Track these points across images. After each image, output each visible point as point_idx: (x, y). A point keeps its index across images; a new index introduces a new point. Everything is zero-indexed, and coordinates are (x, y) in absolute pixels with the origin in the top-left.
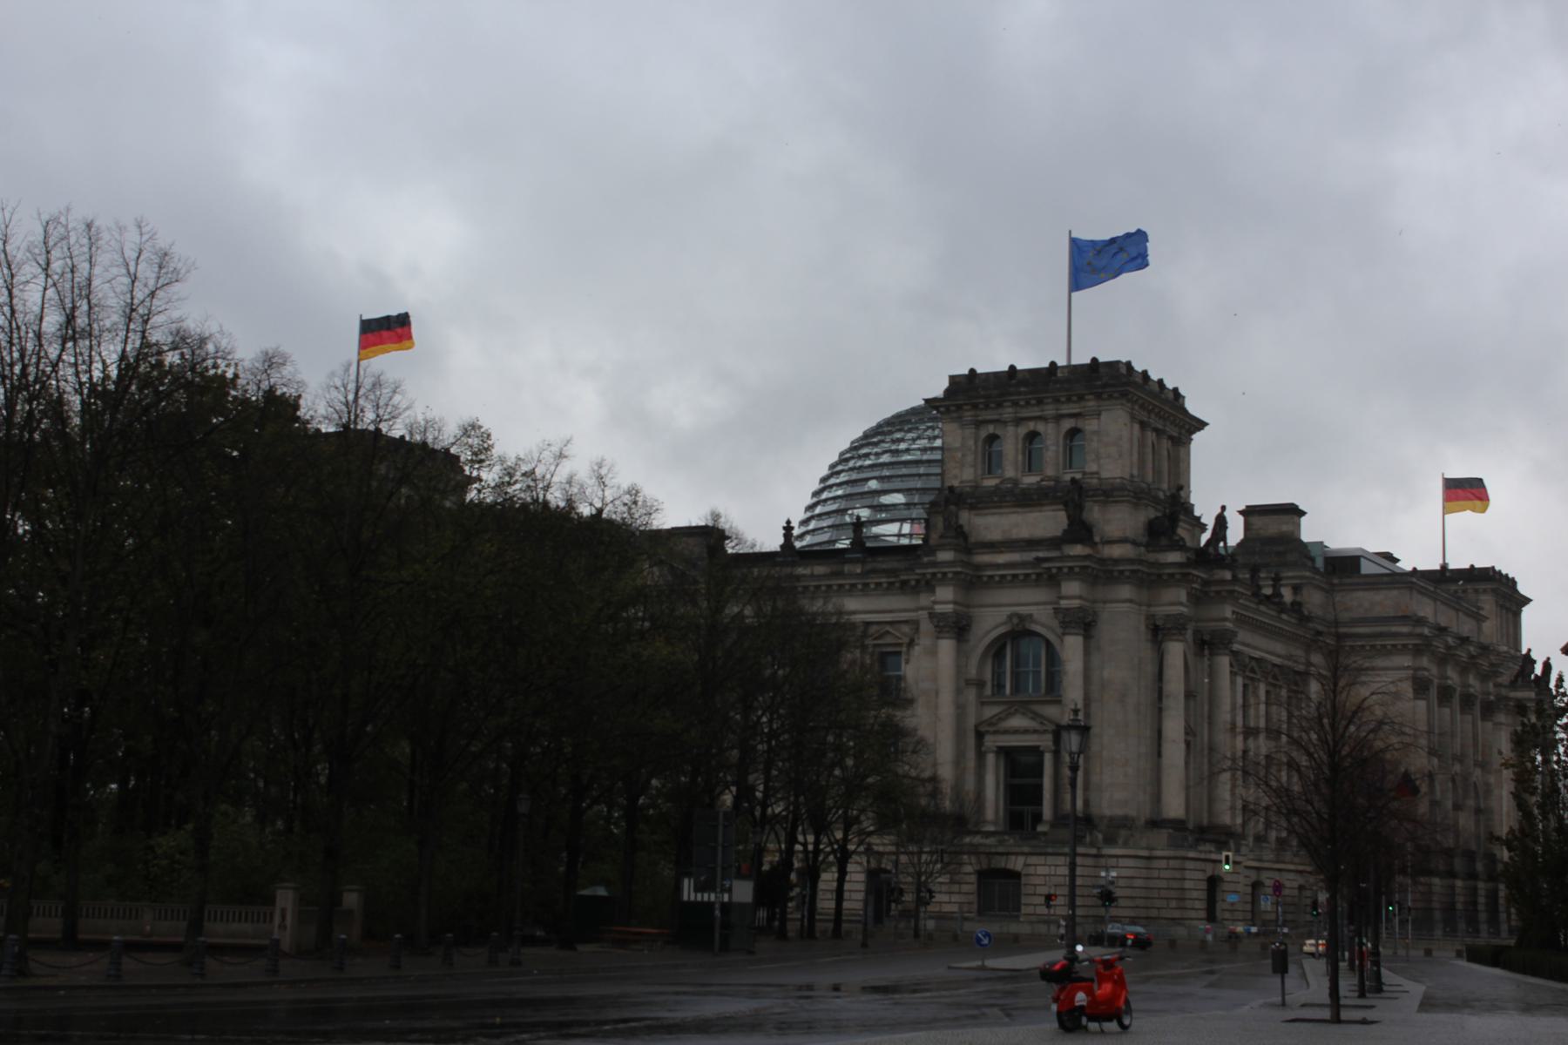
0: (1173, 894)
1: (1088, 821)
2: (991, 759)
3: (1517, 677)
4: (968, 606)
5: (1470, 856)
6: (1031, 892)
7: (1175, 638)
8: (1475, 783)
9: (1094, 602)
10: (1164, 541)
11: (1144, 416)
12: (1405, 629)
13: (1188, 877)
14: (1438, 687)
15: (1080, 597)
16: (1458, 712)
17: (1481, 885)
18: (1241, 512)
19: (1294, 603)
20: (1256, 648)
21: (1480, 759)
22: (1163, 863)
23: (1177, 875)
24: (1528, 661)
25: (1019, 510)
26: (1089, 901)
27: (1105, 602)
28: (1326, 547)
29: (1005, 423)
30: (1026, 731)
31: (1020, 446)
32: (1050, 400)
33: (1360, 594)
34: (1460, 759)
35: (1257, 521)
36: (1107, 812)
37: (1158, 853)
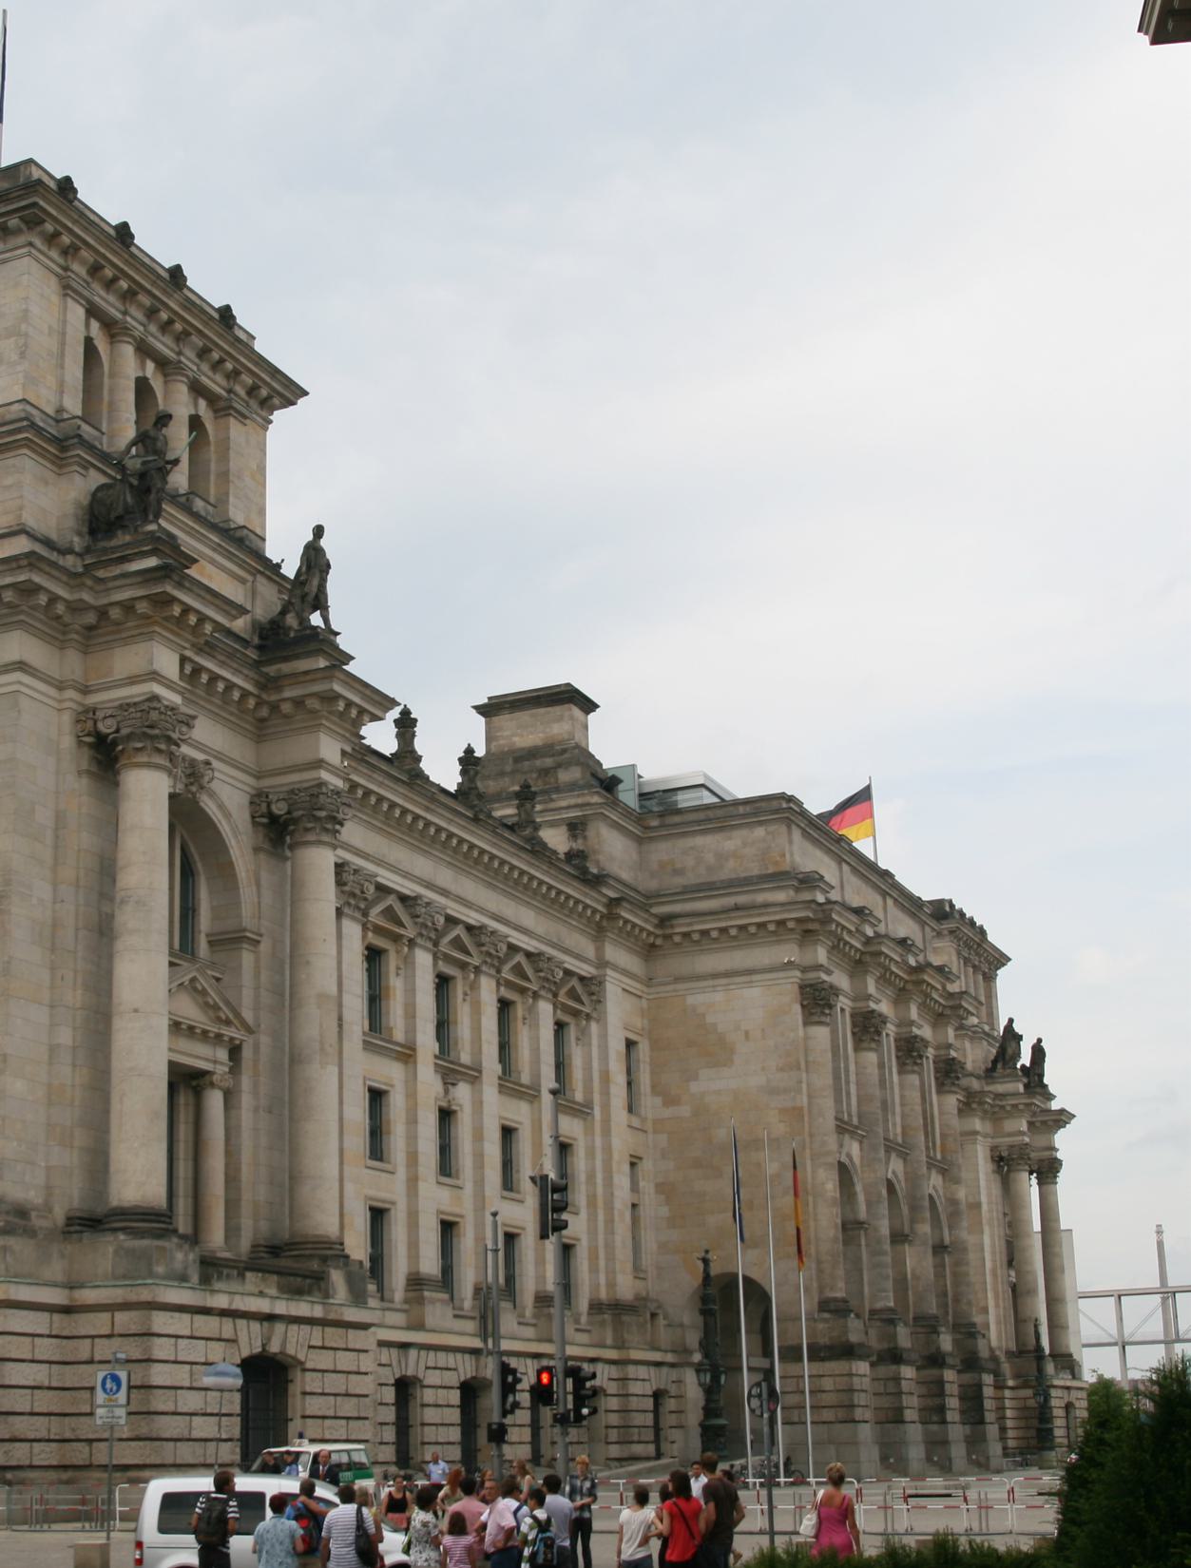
3: (995, 1062)
5: (927, 1325)
7: (143, 758)
8: (930, 1196)
10: (123, 538)
11: (109, 303)
12: (781, 896)
13: (158, 1354)
14: (852, 1016)
16: (895, 1070)
17: (949, 1375)
18: (482, 710)
19: (570, 856)
21: (939, 1157)
22: (100, 1323)
23: (133, 1349)
24: (1012, 1036)
28: (640, 777)
33: (699, 841)
34: (901, 1149)
35: (506, 721)
37: (88, 1296)
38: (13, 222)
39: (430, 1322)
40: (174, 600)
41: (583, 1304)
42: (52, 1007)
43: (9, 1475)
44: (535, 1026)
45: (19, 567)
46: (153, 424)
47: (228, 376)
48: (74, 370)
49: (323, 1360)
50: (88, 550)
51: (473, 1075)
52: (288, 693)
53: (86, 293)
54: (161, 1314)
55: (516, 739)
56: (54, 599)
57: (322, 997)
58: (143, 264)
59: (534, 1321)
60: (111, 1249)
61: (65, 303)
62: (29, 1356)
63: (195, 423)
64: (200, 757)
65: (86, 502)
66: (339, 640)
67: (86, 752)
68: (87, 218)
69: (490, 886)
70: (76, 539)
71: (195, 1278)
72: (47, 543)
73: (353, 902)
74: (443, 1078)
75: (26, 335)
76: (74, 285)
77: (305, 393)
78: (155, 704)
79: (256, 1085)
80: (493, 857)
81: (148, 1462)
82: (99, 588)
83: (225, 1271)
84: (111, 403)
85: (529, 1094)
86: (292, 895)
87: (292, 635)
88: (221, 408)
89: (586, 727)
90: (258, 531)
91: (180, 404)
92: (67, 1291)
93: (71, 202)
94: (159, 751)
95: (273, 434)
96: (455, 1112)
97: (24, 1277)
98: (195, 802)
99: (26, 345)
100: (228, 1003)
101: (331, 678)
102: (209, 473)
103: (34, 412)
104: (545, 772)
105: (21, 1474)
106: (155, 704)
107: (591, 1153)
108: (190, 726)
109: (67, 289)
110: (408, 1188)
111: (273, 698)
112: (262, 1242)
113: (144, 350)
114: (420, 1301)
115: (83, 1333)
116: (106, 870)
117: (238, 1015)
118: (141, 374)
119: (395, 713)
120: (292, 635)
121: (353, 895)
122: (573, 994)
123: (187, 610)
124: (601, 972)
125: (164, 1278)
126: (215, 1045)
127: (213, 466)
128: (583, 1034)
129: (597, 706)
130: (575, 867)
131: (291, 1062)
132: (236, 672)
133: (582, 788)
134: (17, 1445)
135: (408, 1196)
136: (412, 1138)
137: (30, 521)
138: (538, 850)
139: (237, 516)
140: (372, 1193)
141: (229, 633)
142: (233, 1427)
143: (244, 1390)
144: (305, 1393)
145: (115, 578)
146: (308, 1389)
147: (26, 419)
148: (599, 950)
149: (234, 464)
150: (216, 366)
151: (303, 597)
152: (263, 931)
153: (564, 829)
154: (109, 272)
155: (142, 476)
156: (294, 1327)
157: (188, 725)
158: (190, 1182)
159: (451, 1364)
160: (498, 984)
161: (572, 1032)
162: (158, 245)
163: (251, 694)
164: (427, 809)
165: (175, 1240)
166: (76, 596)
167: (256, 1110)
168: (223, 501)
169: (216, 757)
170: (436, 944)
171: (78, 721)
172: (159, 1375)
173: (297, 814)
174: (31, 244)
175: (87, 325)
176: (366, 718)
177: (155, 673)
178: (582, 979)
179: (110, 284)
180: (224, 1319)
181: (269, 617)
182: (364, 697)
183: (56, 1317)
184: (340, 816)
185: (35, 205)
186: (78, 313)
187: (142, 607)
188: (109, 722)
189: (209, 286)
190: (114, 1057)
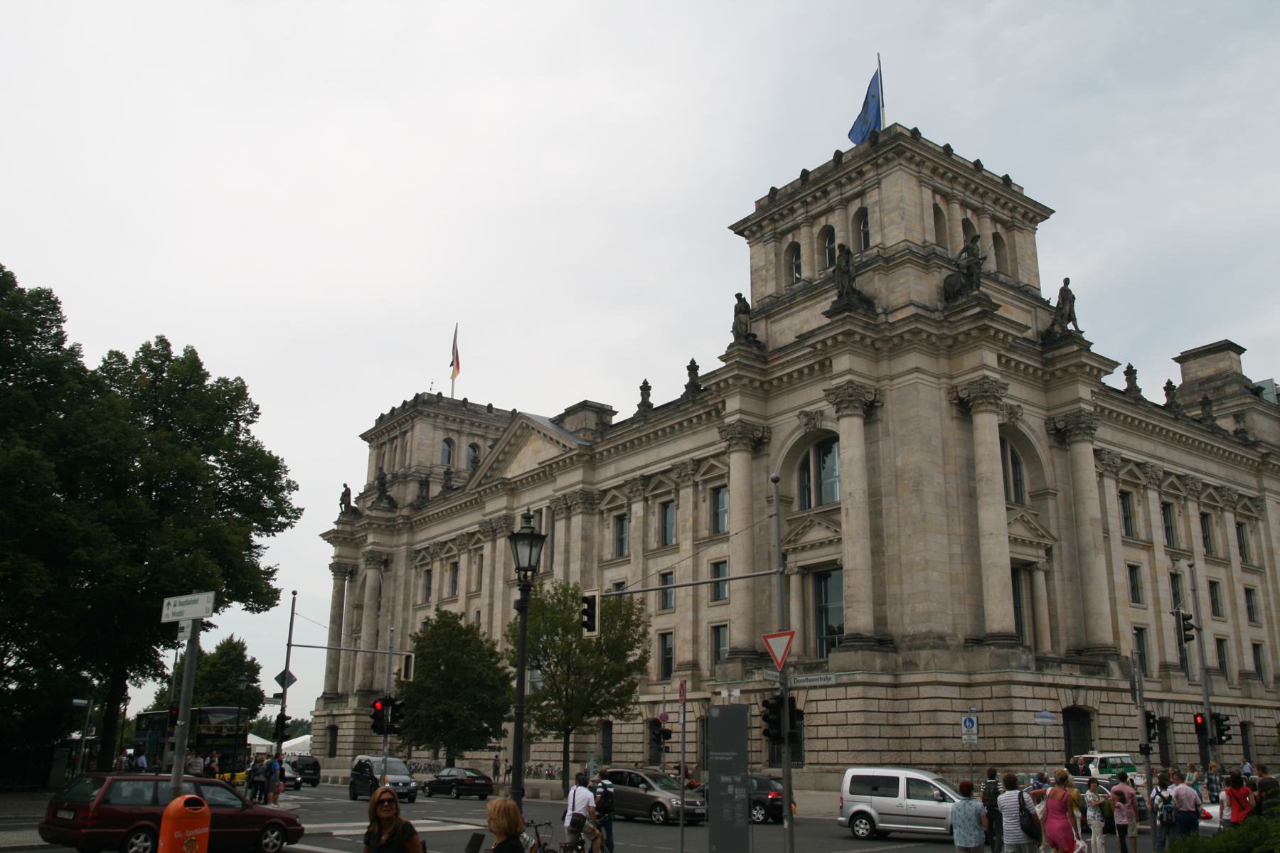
0: (1000, 731)
1: (882, 642)
2: (795, 581)
4: (766, 418)
6: (814, 735)
7: (983, 408)
9: (878, 380)
11: (944, 185)
15: (850, 371)
18: (1177, 360)
19: (1236, 432)
20: (1177, 464)
22: (985, 691)
25: (808, 304)
26: (345, 725)
27: (891, 378)
28: (1276, 385)
29: (796, 227)
30: (822, 544)
31: (816, 246)
32: (832, 186)
36: (910, 630)
37: (978, 678)
38: (890, 155)
39: (1174, 687)
40: (989, 327)
41: (1270, 678)
42: (949, 535)
43: (944, 768)
44: (1224, 526)
45: (911, 322)
46: (972, 238)
47: (1011, 210)
48: (929, 221)
49: (1109, 709)
50: (945, 308)
51: (1189, 554)
52: (1058, 366)
53: (931, 183)
54: (1016, 686)
55: (1198, 373)
56: (930, 335)
57: (1093, 520)
58: (959, 163)
59: (1239, 687)
60: (988, 654)
61: (921, 190)
62: (950, 709)
63: (996, 237)
64: (1015, 403)
65: (942, 285)
66: (1084, 335)
67: (954, 407)
68: (928, 146)
69: (1189, 453)
70: (939, 304)
71: (1033, 668)
72: (925, 308)
73: (1108, 469)
74: (1171, 558)
75: (904, 209)
76: (924, 180)
77: (1054, 212)
78: (986, 380)
79: (1061, 567)
80: (1188, 438)
81: (1014, 762)
82: (953, 326)
83: (1050, 664)
84: (950, 235)
85: (1226, 563)
86: (1072, 469)
87: (1058, 336)
88: (1009, 226)
89: (1240, 362)
90: (1036, 286)
91: (986, 229)
92: (967, 676)
93: (918, 140)
94: (991, 403)
95: (1038, 235)
96: (1180, 575)
97: (945, 669)
98: (1015, 427)
99: (903, 213)
100: (1042, 527)
101: (1080, 356)
102: (1006, 260)
103: (911, 245)
104: (1217, 389)
105: (951, 768)
106: (986, 380)
107: (1266, 594)
108: (1006, 389)
109: (921, 182)
110: (1156, 617)
111: (1052, 369)
112: (1072, 648)
113: (965, 205)
114: (1168, 677)
115: (978, 697)
116: (970, 464)
117: (1048, 532)
118: (964, 217)
119: (1123, 368)
120: (1058, 336)
121: (1109, 465)
122: (1245, 507)
123: (998, 331)
124: (1262, 494)
125: (1016, 668)
126: (1037, 548)
127: (1008, 256)
128: (1255, 530)
129: (1246, 350)
130: (1240, 438)
131: (1079, 555)
132: (1029, 358)
133: (1240, 395)
134: (947, 753)
135: (1156, 621)
136: (1155, 591)
137: (914, 298)
138: (1216, 431)
139: (1024, 279)
140: (1135, 620)
141: (1025, 339)
142: (1061, 744)
143: (1066, 725)
144: (1100, 727)
145: (959, 321)
146: (1101, 724)
147: (907, 249)
148: (1260, 482)
149: (1019, 255)
150: (1004, 206)
151: (1062, 316)
152: (1058, 488)
153: (1232, 418)
154: (941, 170)
155: (968, 268)
156: (1090, 693)
157: (1004, 388)
158: (1031, 619)
159: (1190, 711)
160: (1199, 505)
161: (1248, 528)
162: (966, 151)
163: (1038, 369)
164: (1146, 417)
165: (1021, 649)
166: (941, 332)
167: (1063, 580)
168: (1015, 272)
169: (1024, 403)
170: (1159, 487)
171: (949, 393)
172: (1017, 718)
173: (1070, 427)
174: (901, 164)
175: (934, 198)
176: (1102, 374)
177: (985, 365)
178: (1250, 499)
179: (943, 176)
180: (1051, 689)
181: (1045, 328)
182: (1100, 363)
183: (963, 689)
184: (1093, 426)
185: (900, 145)
186: (928, 193)
187: (974, 333)
188: (964, 392)
189: (995, 167)
190: (982, 558)
